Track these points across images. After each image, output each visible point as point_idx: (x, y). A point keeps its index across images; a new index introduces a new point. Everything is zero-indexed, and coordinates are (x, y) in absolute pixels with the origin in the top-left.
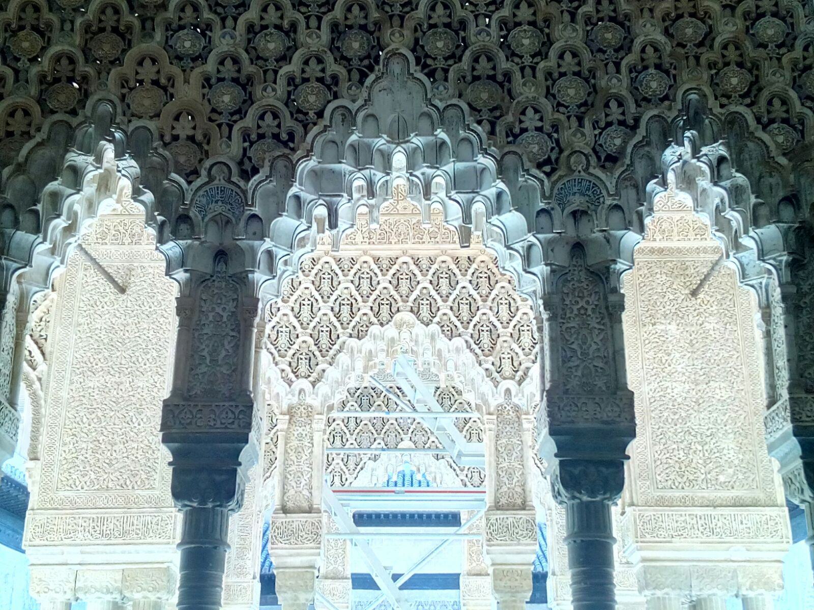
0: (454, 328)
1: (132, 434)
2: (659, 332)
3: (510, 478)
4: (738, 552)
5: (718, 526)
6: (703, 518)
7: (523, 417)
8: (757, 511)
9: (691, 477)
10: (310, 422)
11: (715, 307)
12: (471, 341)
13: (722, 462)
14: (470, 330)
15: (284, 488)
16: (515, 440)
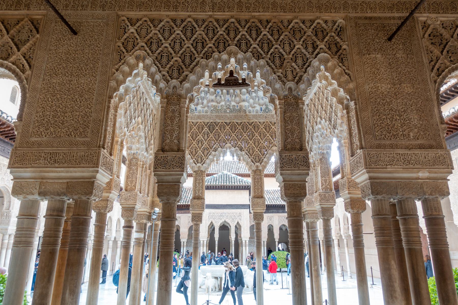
0: (260, 55)
1: (76, 107)
2: (372, 58)
3: (293, 134)
4: (423, 174)
5: (412, 159)
6: (403, 155)
7: (300, 101)
8: (434, 151)
9: (395, 133)
10: (179, 103)
11: (401, 46)
12: (270, 61)
13: (411, 126)
14: (269, 56)
15: (163, 138)
16: (294, 114)
